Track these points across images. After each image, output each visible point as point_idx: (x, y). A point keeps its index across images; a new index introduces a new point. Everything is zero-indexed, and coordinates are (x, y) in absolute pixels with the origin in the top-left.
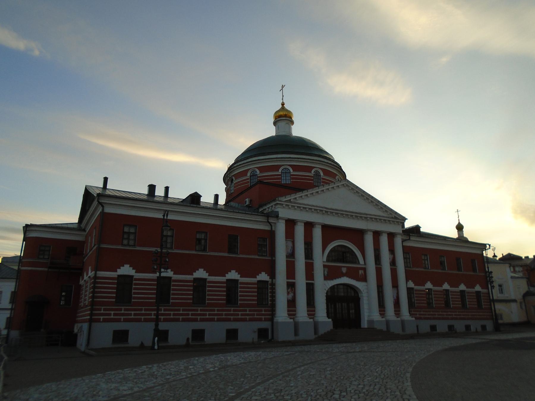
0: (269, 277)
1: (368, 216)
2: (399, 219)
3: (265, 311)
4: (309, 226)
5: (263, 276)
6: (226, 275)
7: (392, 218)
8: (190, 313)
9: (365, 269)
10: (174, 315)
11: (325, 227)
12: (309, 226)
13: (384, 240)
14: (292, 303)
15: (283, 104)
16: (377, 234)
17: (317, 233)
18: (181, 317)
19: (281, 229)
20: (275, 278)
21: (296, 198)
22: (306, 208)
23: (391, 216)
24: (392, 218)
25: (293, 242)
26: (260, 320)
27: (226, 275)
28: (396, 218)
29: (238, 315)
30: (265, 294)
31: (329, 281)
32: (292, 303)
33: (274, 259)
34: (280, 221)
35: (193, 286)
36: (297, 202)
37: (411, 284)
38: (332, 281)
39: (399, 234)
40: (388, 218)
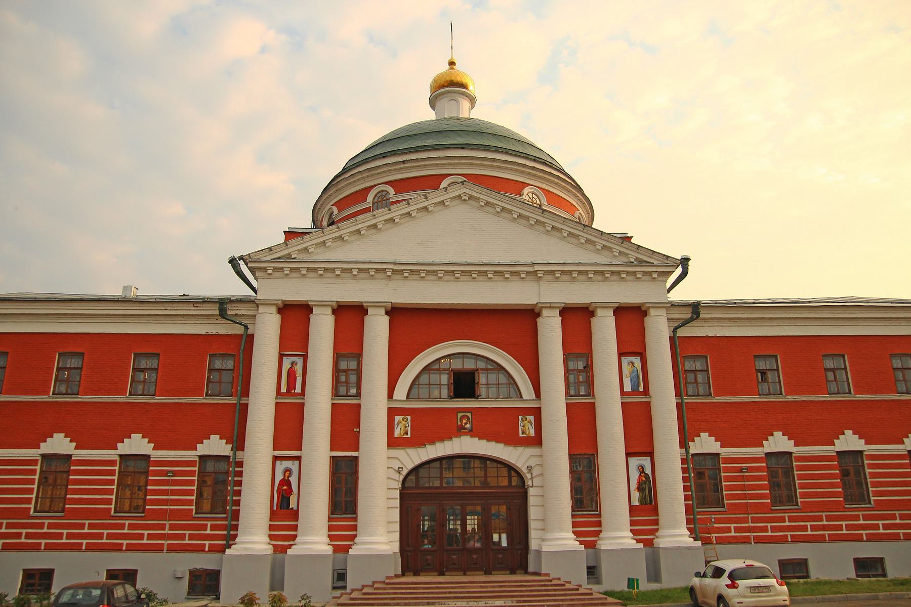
0: (230, 446)
1: (537, 268)
2: (651, 264)
3: (213, 528)
4: (350, 316)
5: (215, 446)
6: (119, 445)
7: (631, 264)
8: (24, 531)
9: (537, 413)
10: (69, 536)
11: (395, 312)
12: (350, 316)
13: (605, 330)
14: (284, 510)
15: (452, 63)
16: (577, 318)
17: (377, 329)
18: (85, 542)
19: (268, 330)
20: (243, 449)
21: (306, 249)
22: (350, 270)
23: (626, 260)
24: (631, 264)
25: (305, 357)
26: (200, 549)
27: (119, 445)
28: (641, 262)
29: (141, 537)
30: (219, 487)
31: (411, 451)
32: (284, 510)
33: (244, 400)
34: (262, 309)
35: (69, 472)
36: (314, 258)
37: (705, 444)
38: (421, 451)
39: (658, 305)
40: (611, 265)
